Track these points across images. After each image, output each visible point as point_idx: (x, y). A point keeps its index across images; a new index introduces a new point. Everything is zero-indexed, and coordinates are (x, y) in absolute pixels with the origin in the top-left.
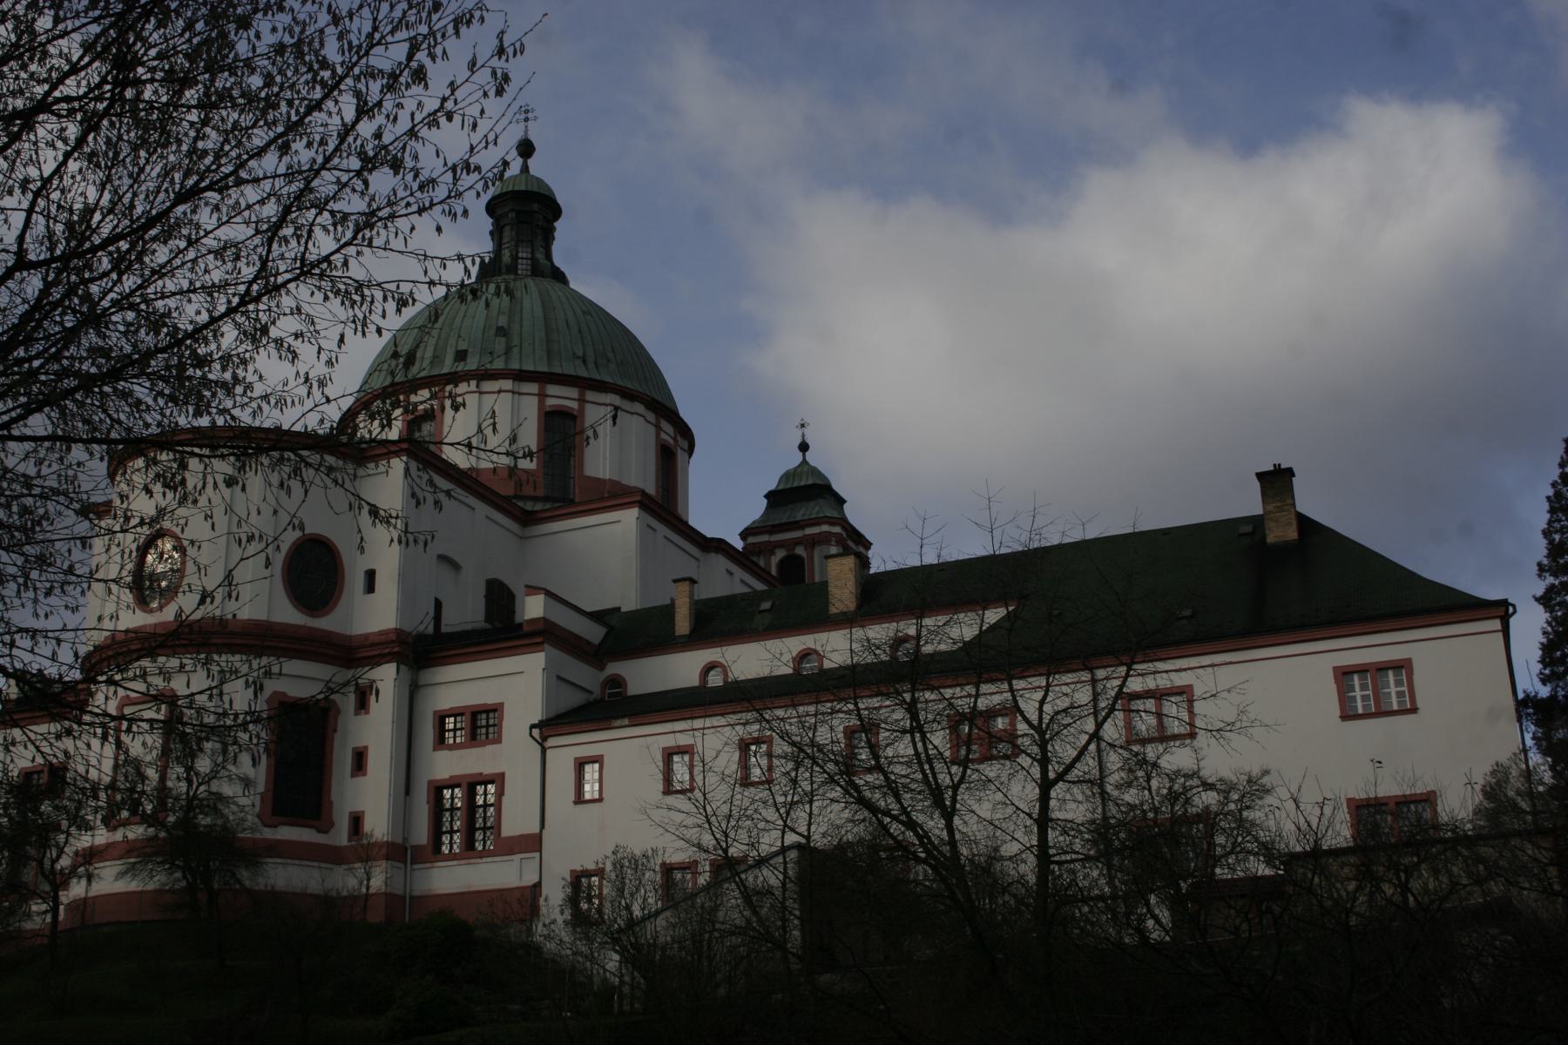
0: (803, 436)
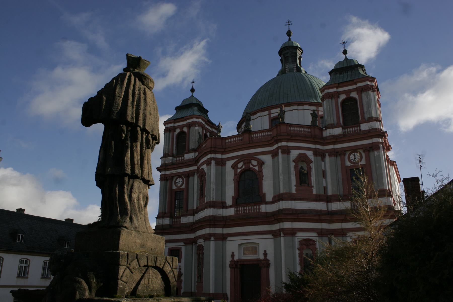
0: (193, 87)
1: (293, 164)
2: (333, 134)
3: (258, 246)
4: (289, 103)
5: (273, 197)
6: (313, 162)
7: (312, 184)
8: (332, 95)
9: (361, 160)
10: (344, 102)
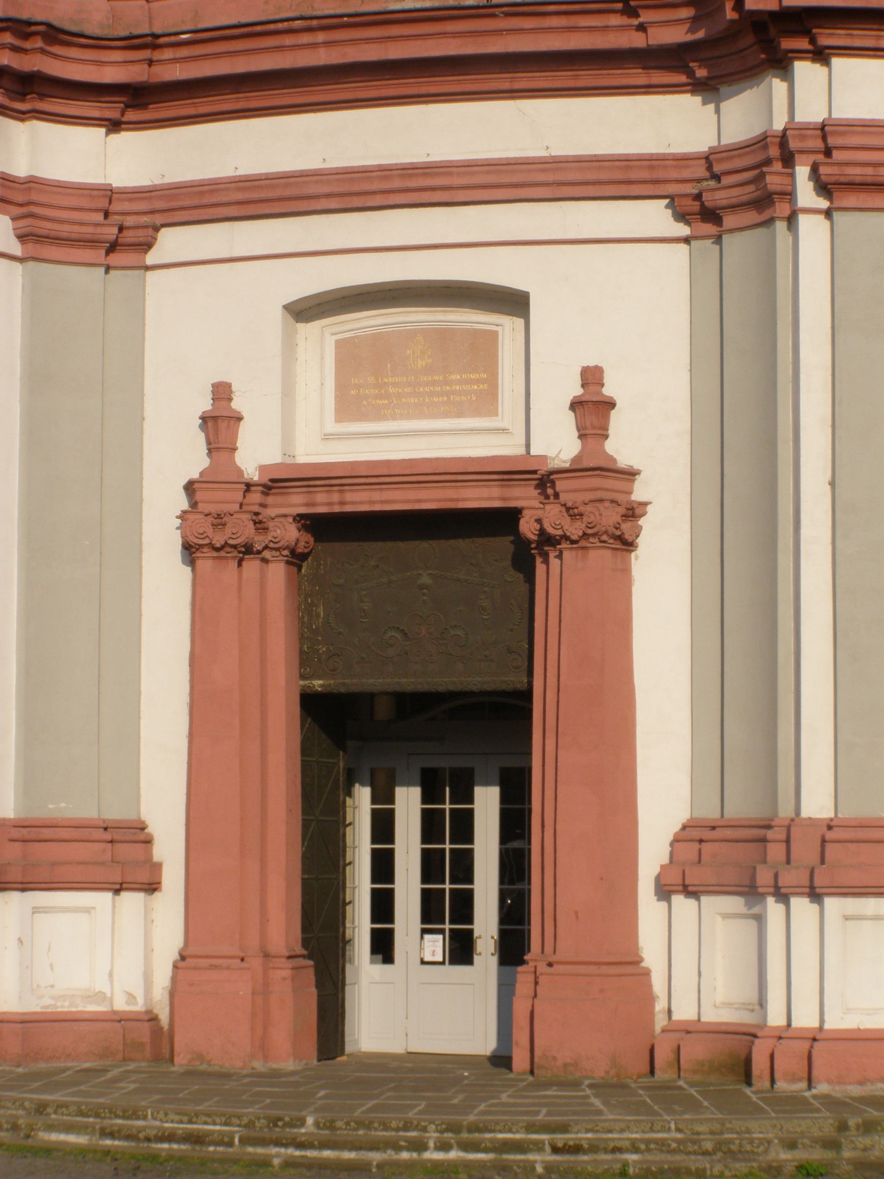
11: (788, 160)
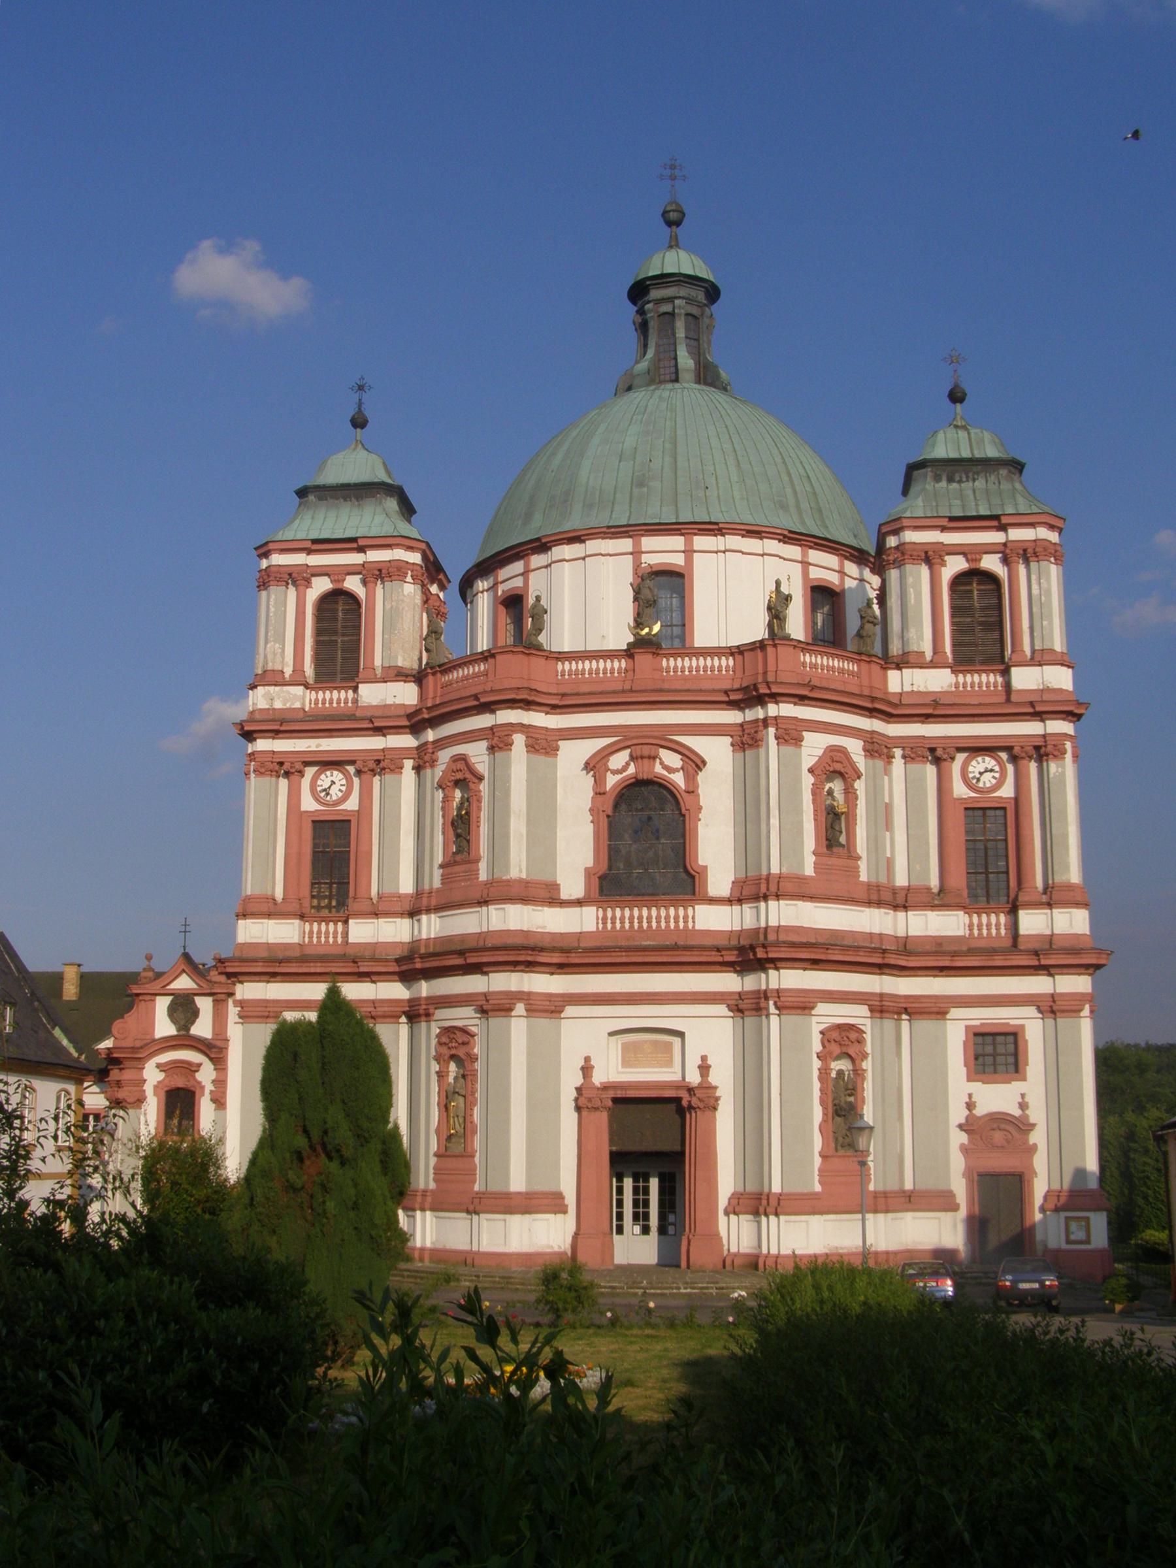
0: (360, 404)
1: (808, 781)
2: (922, 689)
3: (677, 1041)
4: (717, 524)
5: (733, 882)
6: (863, 777)
7: (859, 850)
8: (926, 553)
9: (1000, 783)
10: (960, 580)
11: (766, 998)
